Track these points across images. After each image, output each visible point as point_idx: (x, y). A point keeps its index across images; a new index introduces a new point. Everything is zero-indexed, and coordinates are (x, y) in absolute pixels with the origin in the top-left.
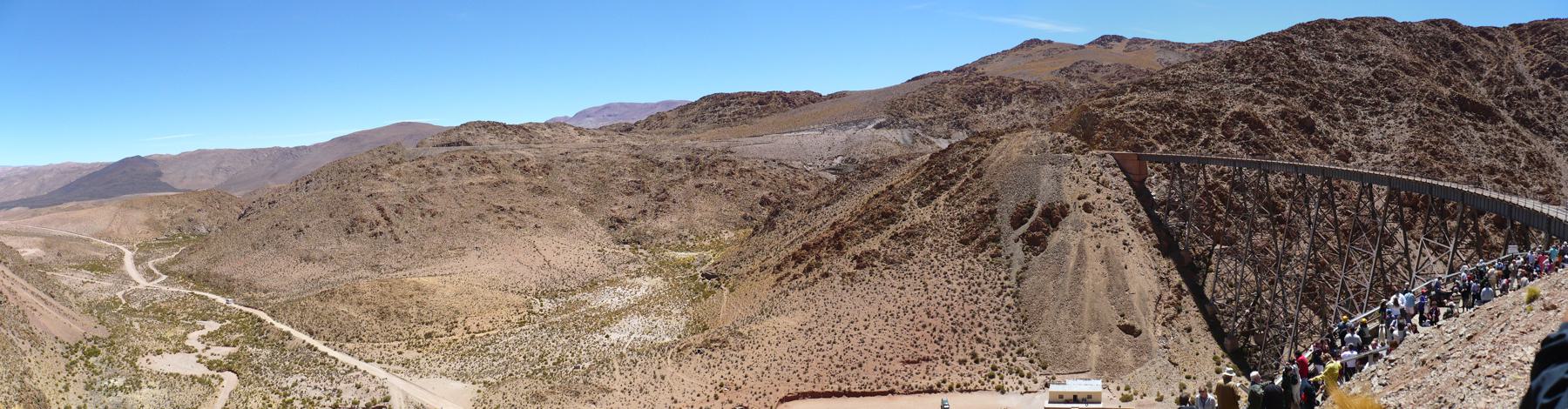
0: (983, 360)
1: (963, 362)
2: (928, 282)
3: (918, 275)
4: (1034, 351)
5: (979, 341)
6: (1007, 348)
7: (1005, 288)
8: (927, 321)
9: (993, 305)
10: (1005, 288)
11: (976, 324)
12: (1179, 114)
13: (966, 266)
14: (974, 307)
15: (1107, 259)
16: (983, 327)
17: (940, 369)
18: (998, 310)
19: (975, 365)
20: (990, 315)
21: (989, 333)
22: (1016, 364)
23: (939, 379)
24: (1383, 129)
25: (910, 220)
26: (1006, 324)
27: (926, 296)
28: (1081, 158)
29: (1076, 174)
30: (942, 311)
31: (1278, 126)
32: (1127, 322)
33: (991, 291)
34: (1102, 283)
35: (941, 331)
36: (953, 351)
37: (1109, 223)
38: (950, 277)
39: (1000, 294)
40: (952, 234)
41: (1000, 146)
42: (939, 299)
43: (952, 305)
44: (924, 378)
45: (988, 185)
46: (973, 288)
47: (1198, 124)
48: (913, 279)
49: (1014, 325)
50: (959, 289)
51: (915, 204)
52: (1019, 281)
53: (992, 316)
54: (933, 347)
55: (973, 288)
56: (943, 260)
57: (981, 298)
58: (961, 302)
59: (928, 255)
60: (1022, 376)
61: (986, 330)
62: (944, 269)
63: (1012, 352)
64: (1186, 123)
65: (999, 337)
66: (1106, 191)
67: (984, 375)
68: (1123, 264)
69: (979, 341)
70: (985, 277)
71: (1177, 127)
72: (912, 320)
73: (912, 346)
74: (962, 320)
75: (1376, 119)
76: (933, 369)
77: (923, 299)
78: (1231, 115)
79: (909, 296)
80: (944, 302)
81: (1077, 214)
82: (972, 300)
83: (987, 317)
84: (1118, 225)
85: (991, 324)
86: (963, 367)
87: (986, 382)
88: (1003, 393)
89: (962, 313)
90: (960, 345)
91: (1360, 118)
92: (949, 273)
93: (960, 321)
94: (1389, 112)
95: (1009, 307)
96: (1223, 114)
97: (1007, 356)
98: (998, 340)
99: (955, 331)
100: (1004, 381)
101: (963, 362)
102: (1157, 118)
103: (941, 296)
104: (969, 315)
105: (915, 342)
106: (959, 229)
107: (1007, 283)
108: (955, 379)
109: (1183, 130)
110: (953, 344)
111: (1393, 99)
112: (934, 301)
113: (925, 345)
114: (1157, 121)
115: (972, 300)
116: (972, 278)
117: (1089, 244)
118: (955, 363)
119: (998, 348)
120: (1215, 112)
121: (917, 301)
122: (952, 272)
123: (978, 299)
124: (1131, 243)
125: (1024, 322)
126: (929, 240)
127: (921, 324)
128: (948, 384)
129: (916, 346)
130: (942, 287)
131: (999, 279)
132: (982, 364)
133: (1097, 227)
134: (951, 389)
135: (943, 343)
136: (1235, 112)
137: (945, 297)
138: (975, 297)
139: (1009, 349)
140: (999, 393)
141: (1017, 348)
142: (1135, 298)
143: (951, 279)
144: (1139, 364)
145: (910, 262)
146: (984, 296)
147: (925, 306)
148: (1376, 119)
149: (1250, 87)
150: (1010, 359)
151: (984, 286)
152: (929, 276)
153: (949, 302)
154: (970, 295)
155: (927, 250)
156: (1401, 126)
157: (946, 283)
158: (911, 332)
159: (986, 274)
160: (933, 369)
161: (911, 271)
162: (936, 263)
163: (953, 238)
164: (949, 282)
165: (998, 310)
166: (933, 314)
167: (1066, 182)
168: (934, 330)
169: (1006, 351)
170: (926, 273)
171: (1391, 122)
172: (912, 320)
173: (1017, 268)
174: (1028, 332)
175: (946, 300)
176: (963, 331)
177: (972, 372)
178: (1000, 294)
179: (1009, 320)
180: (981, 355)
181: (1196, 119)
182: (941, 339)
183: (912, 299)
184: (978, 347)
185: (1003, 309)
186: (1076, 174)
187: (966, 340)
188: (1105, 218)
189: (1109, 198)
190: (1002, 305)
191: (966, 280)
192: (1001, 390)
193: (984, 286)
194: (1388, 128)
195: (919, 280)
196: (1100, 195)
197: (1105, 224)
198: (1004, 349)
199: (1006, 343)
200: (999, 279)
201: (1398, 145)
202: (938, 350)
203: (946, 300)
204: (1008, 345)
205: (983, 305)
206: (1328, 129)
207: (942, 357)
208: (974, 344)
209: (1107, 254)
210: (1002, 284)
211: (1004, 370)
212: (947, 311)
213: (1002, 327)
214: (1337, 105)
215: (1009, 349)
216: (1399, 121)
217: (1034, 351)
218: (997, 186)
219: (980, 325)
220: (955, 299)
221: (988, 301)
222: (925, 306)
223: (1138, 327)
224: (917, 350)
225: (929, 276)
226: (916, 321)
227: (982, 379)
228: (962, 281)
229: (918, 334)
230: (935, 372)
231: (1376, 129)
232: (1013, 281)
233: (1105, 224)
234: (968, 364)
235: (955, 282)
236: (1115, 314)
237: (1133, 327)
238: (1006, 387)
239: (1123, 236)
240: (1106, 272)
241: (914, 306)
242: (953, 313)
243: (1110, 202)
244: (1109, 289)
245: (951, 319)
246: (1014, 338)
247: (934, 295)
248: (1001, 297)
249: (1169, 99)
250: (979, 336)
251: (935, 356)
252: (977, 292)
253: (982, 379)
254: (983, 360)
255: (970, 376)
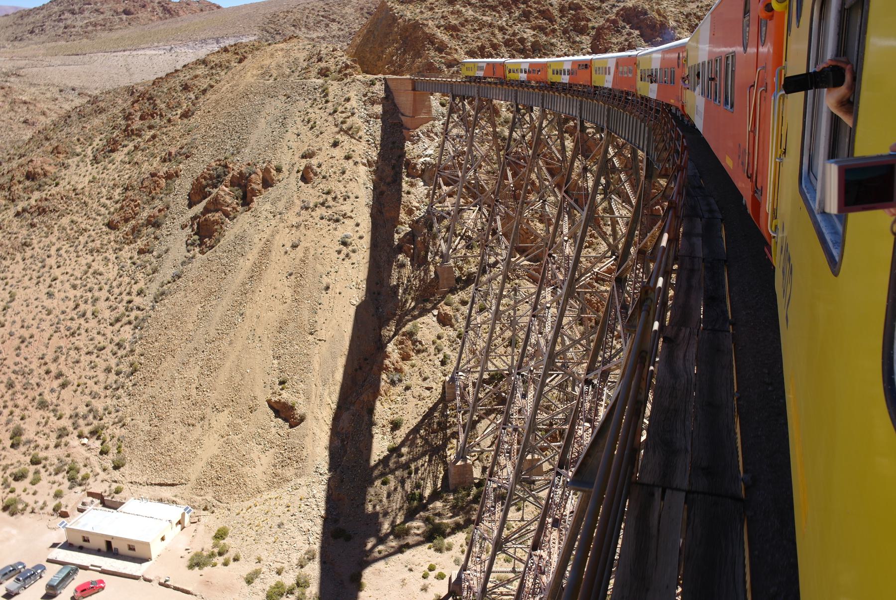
12: (524, 11)
28: (334, 88)
29: (316, 114)
47: (554, 31)
52: (160, 297)
64: (533, 28)
71: (514, 34)
78: (617, 14)
81: (289, 183)
84: (346, 208)
96: (606, 12)
102: (485, 18)
109: (522, 41)
114: (482, 25)
120: (592, 8)
133: (307, 208)
136: (624, 9)
144: (276, 481)
173: (167, 272)
181: (552, 20)
186: (316, 114)
189: (348, 158)
197: (323, 204)
223: (300, 410)
237: (292, 408)
239: (346, 229)
240: (288, 293)
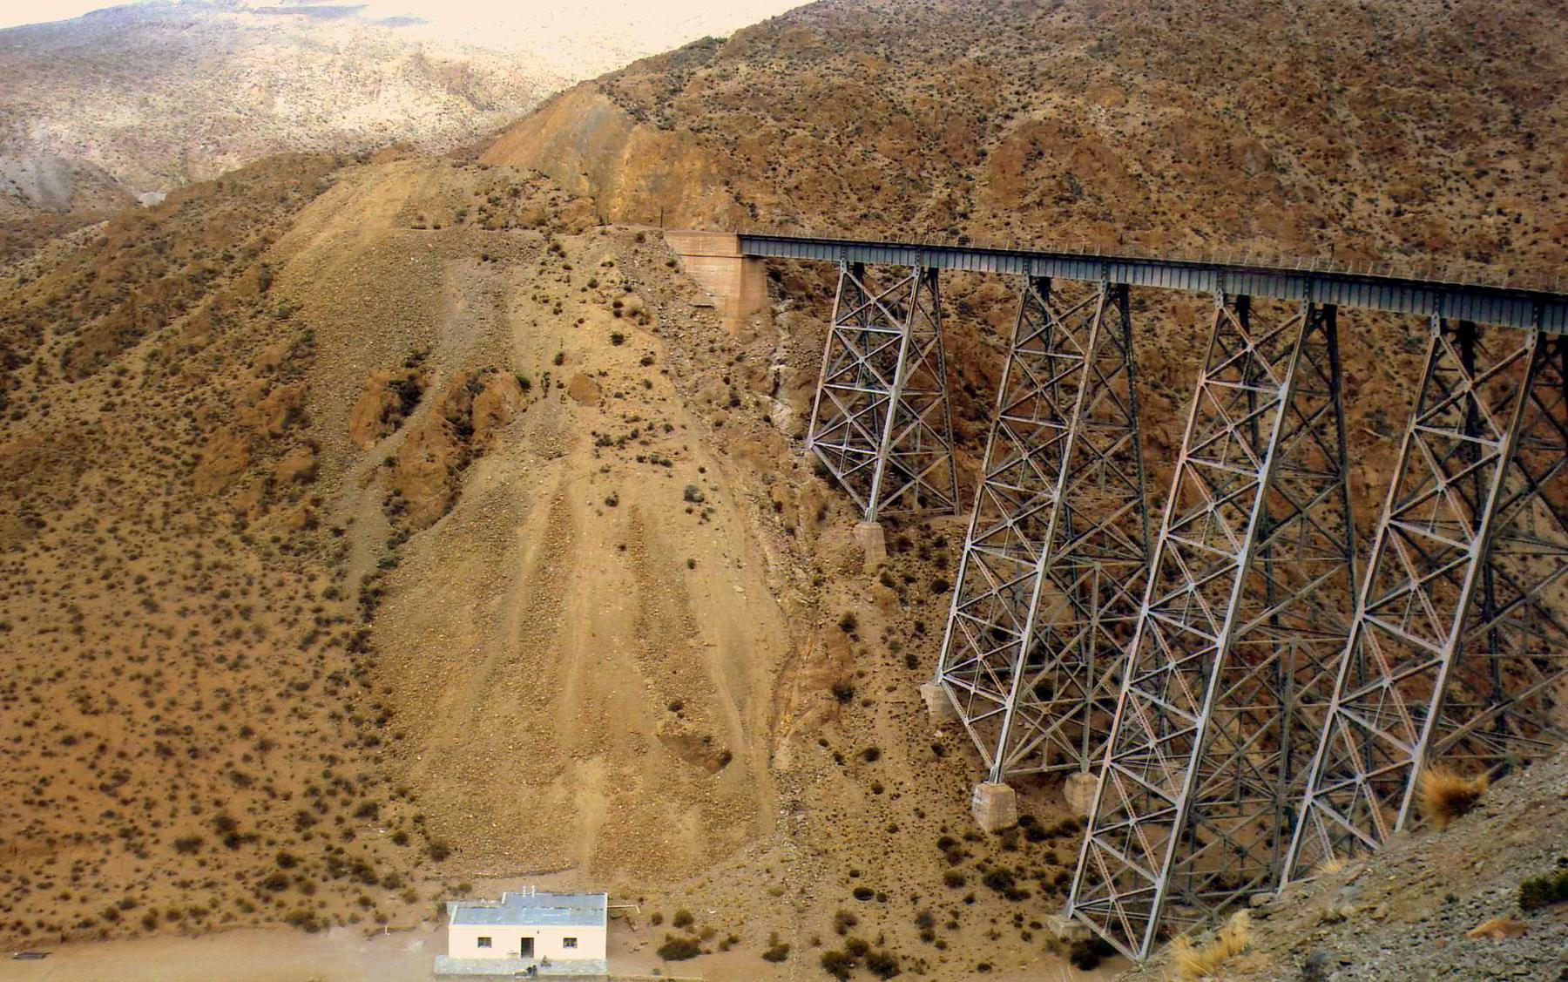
0: (252, 838)
1: (188, 846)
2: (85, 606)
3: (52, 588)
4: (410, 811)
5: (241, 780)
6: (328, 800)
7: (328, 622)
8: (79, 724)
9: (289, 673)
10: (328, 622)
11: (234, 730)
13: (208, 559)
14: (229, 680)
15: (634, 542)
16: (255, 740)
17: (119, 867)
18: (303, 687)
19: (226, 854)
20: (277, 703)
21: (275, 760)
22: (353, 850)
23: (112, 900)
24: (1484, 186)
25: (34, 416)
26: (327, 728)
27: (78, 649)
30: (128, 693)
31: (1157, 168)
32: (689, 727)
33: (281, 632)
34: (621, 608)
35: (122, 755)
36: (159, 813)
37: (644, 436)
38: (155, 590)
39: (310, 640)
40: (168, 459)
41: (328, 199)
42: (119, 659)
43: (159, 674)
44: (66, 897)
45: (284, 316)
46: (229, 625)
48: (36, 597)
49: (350, 731)
50: (183, 627)
51: (56, 371)
53: (283, 707)
54: (95, 804)
55: (229, 625)
56: (135, 540)
57: (251, 655)
58: (188, 665)
59: (89, 525)
60: (371, 881)
61: (265, 746)
62: (139, 567)
63: (344, 812)
65: (303, 769)
66: (642, 340)
67: (253, 882)
68: (683, 559)
69: (241, 780)
70: (265, 591)
72: (29, 724)
73: (29, 802)
74: (186, 718)
75: (1461, 155)
76: (96, 871)
77: (67, 660)
79: (21, 650)
80: (132, 669)
82: (222, 659)
83: (269, 710)
85: (281, 729)
86: (190, 861)
87: (258, 904)
88: (313, 929)
89: (191, 698)
90: (183, 794)
91: (1412, 150)
92: (154, 578)
93: (184, 723)
94: (1505, 133)
95: (336, 678)
97: (327, 825)
98: (301, 777)
99: (165, 752)
100: (316, 899)
101: (188, 846)
103: (126, 650)
104: (211, 704)
105: (39, 792)
106: (190, 443)
107: (332, 609)
108: (163, 895)
110: (159, 793)
111: (1509, 94)
112: (102, 665)
113: (71, 799)
115: (222, 659)
116: (225, 595)
117: (586, 496)
118: (162, 853)
119: (300, 803)
121: (41, 663)
122: (163, 576)
123: (241, 657)
124: (709, 495)
125: (381, 722)
126: (94, 478)
127: (60, 735)
128: (142, 912)
129: (42, 804)
130: (129, 621)
131: (309, 596)
132: (248, 849)
134: (150, 923)
135: (126, 791)
137: (137, 651)
138: (233, 649)
139: (334, 804)
140: (300, 932)
141: (357, 802)
142: (716, 661)
143: (156, 599)
145: (32, 548)
146: (263, 649)
147: (72, 680)
148: (1461, 155)
149: (1079, 50)
150: (335, 832)
151: (259, 618)
152: (87, 590)
153: (147, 669)
154: (218, 643)
155: (86, 509)
156: (1544, 178)
157: (142, 611)
158: (26, 762)
159: (269, 583)
160: (96, 871)
161: (32, 575)
162: (112, 549)
163: (170, 474)
164: (152, 607)
165: (303, 687)
166: (100, 703)
167: (522, 310)
168: (102, 748)
169: (325, 810)
170: (78, 582)
171: (1512, 164)
172: (29, 724)
173: (362, 564)
174: (394, 753)
175: (142, 660)
176: (194, 753)
177: (218, 875)
178: (310, 640)
179: (335, 717)
180: (246, 826)
182: (122, 778)
183: (35, 659)
184: (239, 804)
185: (318, 687)
187: (202, 781)
188: (636, 419)
189: (646, 362)
190: (316, 675)
191: (206, 600)
192: (306, 923)
193: (259, 618)
194: (1504, 180)
195: (56, 602)
196: (621, 352)
198: (317, 805)
199: (324, 785)
200: (309, 596)
201: (1532, 236)
202: (110, 814)
203: (142, 660)
204: (332, 793)
205: (258, 676)
206: (1313, 182)
207: (125, 834)
208: (227, 790)
209: (636, 525)
210: (318, 610)
211: (317, 867)
212: (145, 694)
213: (313, 740)
214: (1342, 113)
215: (334, 804)
216: (1535, 160)
217: (410, 811)
218: (312, 319)
219: (246, 732)
220: (169, 656)
221: (274, 664)
222: (72, 680)
224: (43, 814)
225: (87, 590)
226: (44, 726)
227: (248, 896)
228: (193, 602)
229: (48, 767)
230: (100, 878)
231: (1463, 186)
232: (349, 606)
233: (635, 435)
234: (204, 853)
235: (170, 607)
236: (655, 701)
238: (321, 914)
239: (685, 474)
241: (37, 681)
242: (161, 698)
243: (652, 374)
244: (641, 627)
245: (157, 718)
246: (349, 772)
247: (102, 647)
248: (314, 651)
249: (837, 80)
250: (243, 768)
251: (101, 830)
252: (238, 634)
253: (248, 896)
254: (252, 838)
255: (210, 885)
